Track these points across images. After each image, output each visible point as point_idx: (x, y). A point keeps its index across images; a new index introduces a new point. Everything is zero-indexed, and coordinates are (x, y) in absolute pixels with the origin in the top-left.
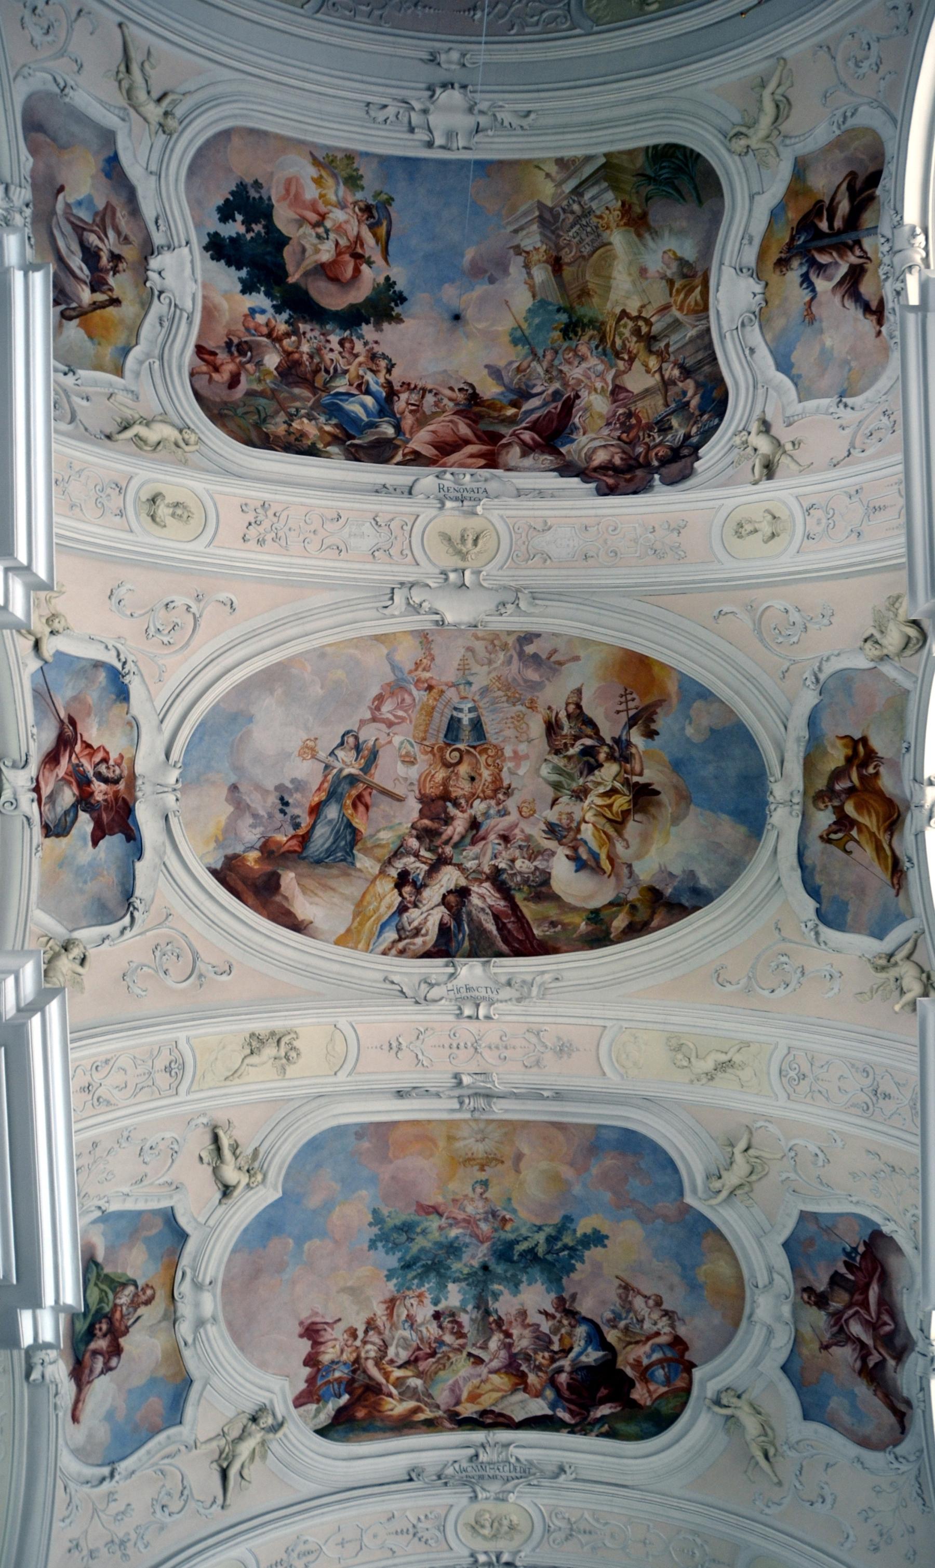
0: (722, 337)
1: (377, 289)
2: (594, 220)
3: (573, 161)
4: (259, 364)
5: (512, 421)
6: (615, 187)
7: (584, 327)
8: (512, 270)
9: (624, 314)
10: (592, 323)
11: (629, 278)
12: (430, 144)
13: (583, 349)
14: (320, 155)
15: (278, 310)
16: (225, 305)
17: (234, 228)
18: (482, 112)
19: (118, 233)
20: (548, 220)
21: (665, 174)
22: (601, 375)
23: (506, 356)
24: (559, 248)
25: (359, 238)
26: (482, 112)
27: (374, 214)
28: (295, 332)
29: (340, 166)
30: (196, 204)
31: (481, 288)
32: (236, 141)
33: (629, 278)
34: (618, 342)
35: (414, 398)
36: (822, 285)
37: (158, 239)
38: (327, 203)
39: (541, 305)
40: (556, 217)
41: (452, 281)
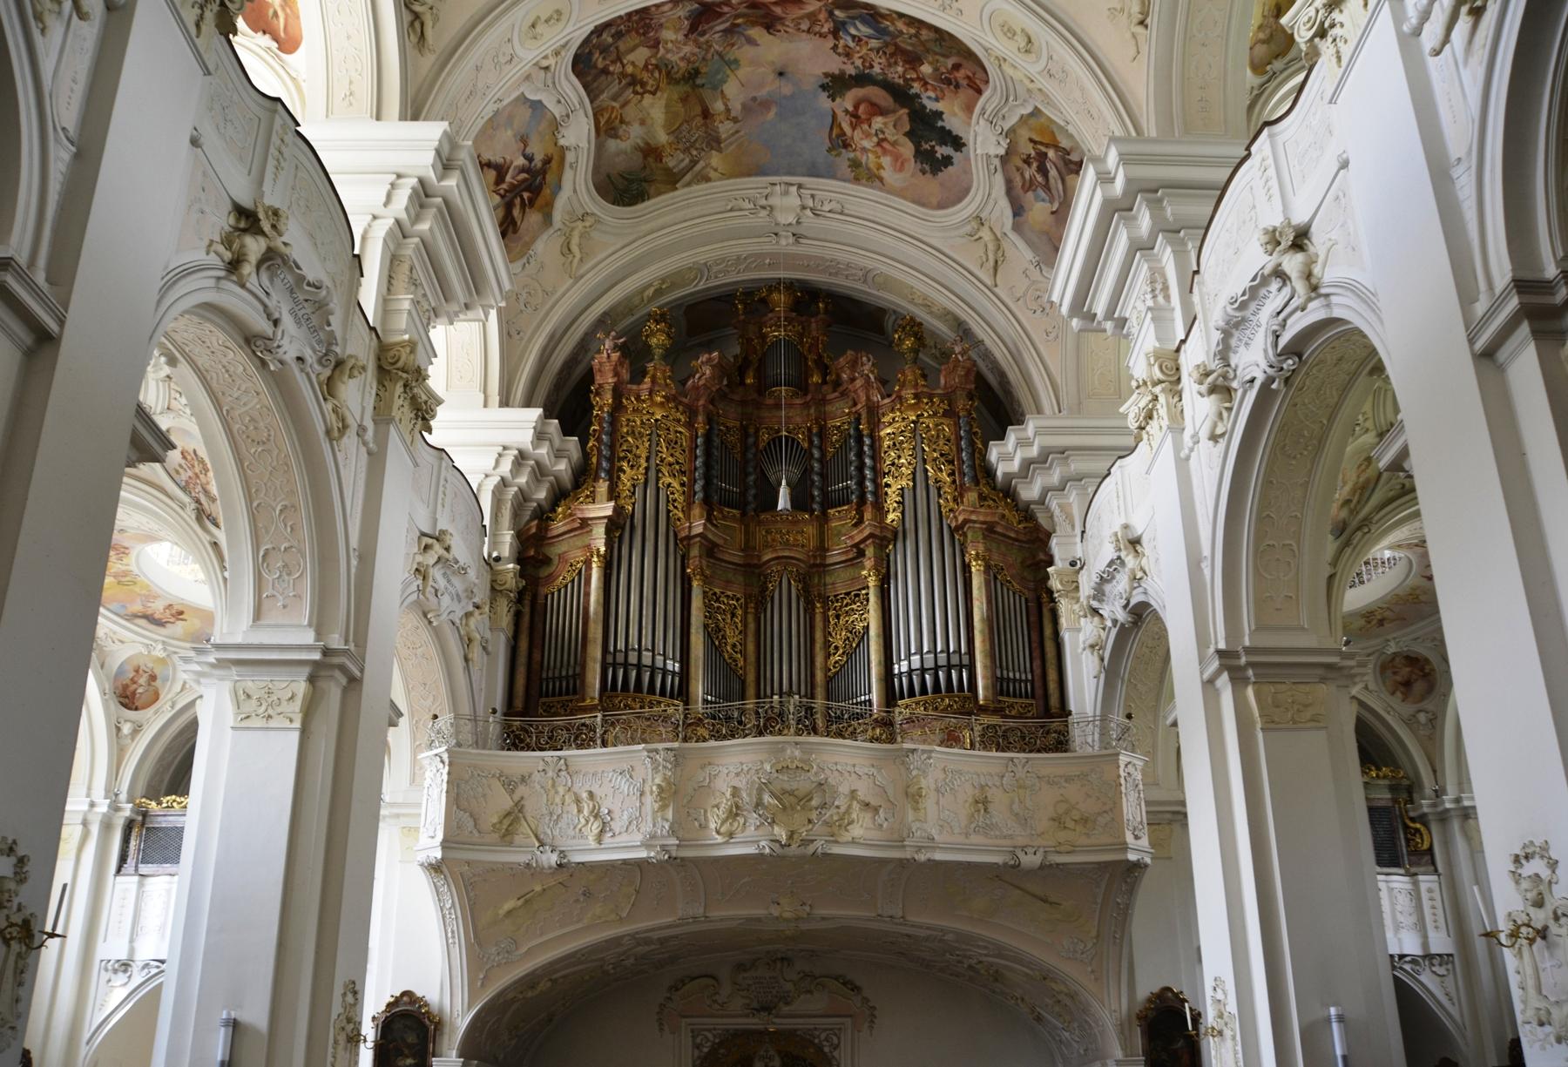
0: (581, 102)
1: (842, 95)
2: (681, 146)
3: (699, 182)
4: (936, 70)
5: (737, 17)
6: (668, 171)
7: (684, 77)
8: (739, 107)
9: (654, 93)
10: (677, 82)
11: (653, 116)
12: (800, 186)
13: (682, 64)
14: (877, 183)
15: (918, 96)
16: (956, 109)
17: (942, 151)
18: (763, 207)
19: (1022, 175)
20: (714, 142)
21: (635, 186)
22: (668, 51)
23: (744, 52)
24: (705, 125)
25: (854, 129)
26: (763, 207)
27: (841, 142)
28: (906, 80)
29: (862, 174)
30: (967, 171)
31: (762, 93)
32: (934, 201)
33: (653, 116)
34: (657, 74)
35: (817, 29)
36: (520, 161)
37: (997, 162)
38: (875, 153)
39: (717, 87)
40: (708, 144)
41: (785, 97)
